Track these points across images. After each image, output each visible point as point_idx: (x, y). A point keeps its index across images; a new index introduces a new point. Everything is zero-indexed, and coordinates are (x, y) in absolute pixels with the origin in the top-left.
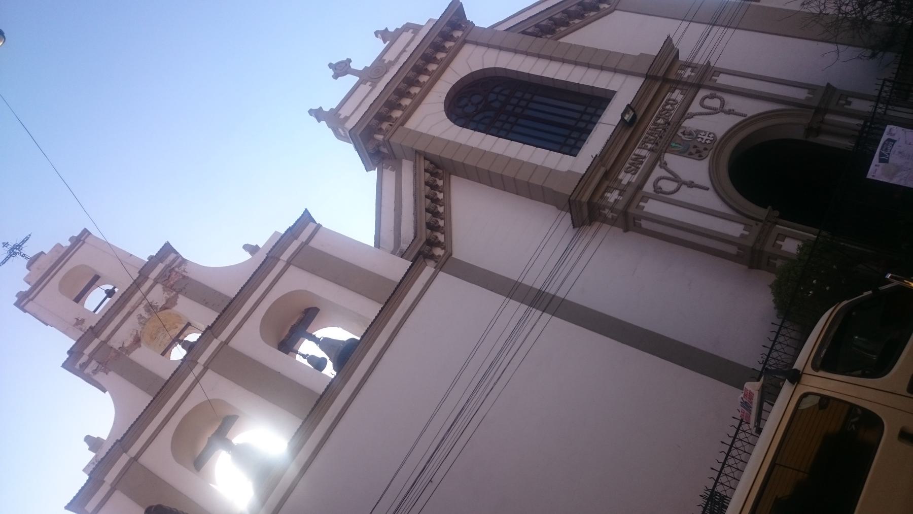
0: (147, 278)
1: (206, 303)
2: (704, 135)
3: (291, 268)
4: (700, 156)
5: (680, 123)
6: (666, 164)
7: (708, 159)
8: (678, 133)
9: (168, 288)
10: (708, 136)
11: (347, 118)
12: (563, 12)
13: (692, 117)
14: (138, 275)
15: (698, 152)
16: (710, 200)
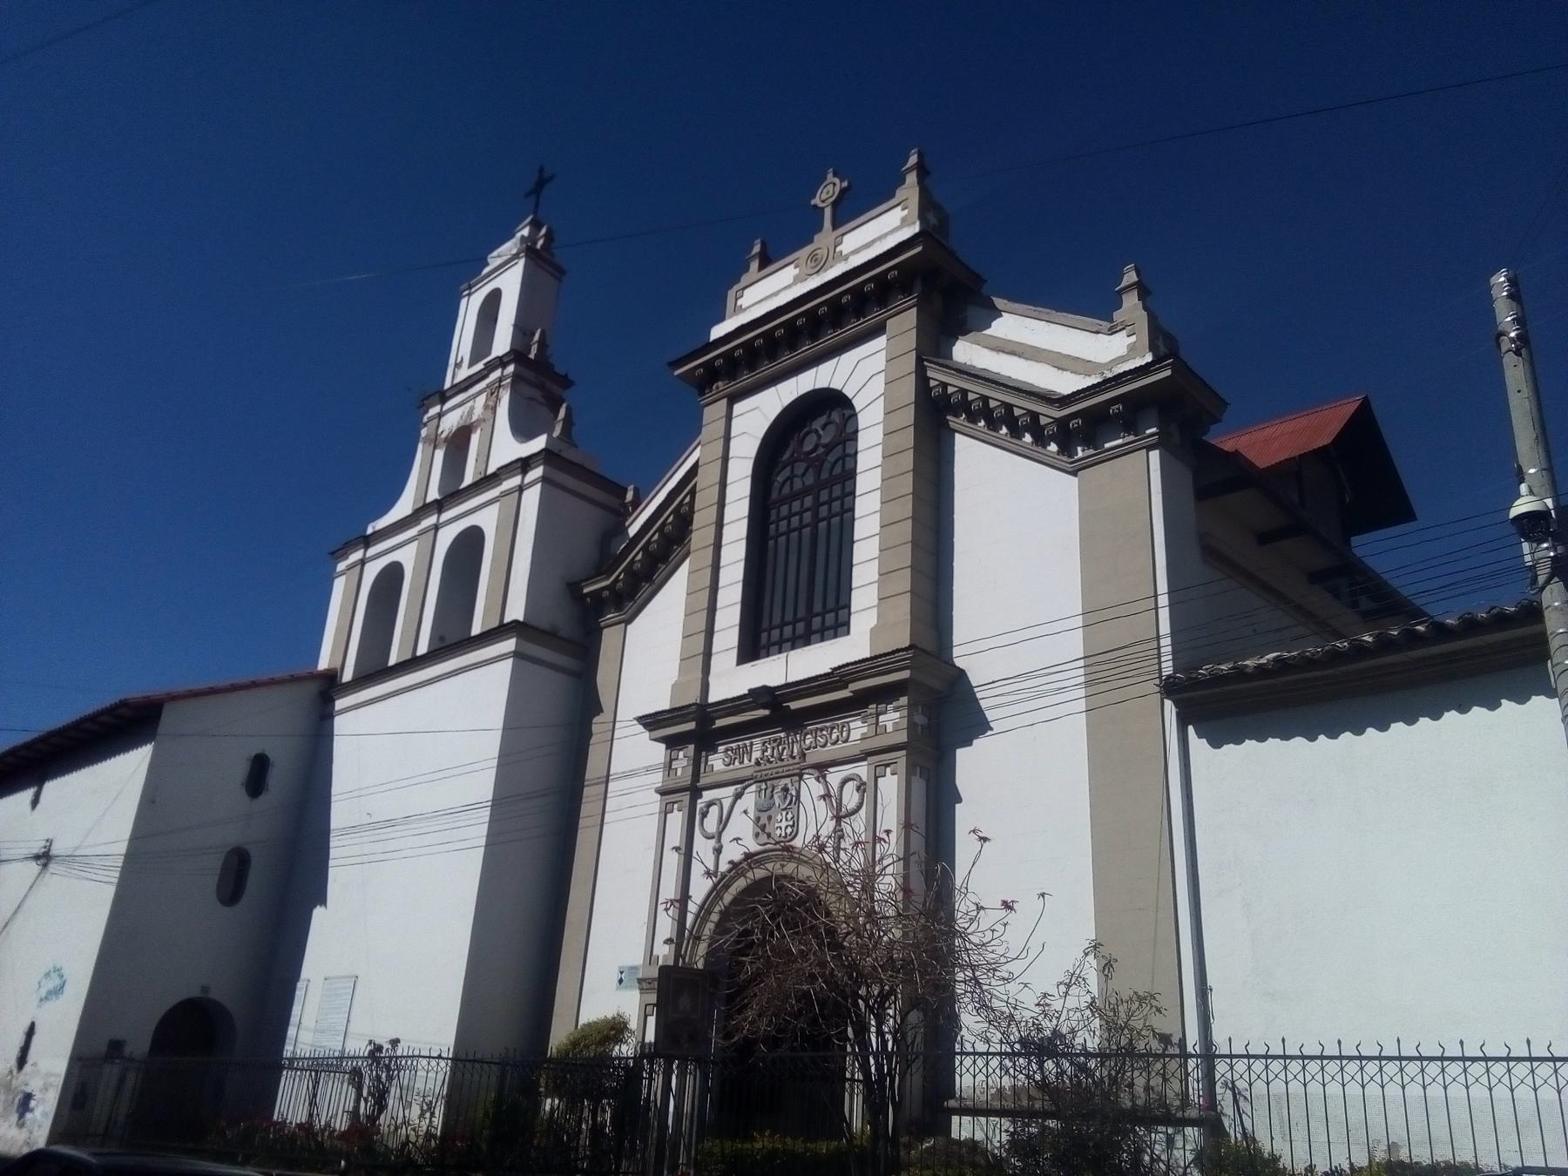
0: (486, 376)
1: (477, 460)
2: (787, 820)
3: (498, 504)
4: (757, 835)
5: (806, 771)
6: (740, 798)
7: (759, 848)
8: (783, 780)
9: (486, 407)
10: (787, 827)
11: (738, 310)
12: (1003, 403)
13: (819, 782)
14: (483, 367)
15: (763, 828)
16: (700, 888)
